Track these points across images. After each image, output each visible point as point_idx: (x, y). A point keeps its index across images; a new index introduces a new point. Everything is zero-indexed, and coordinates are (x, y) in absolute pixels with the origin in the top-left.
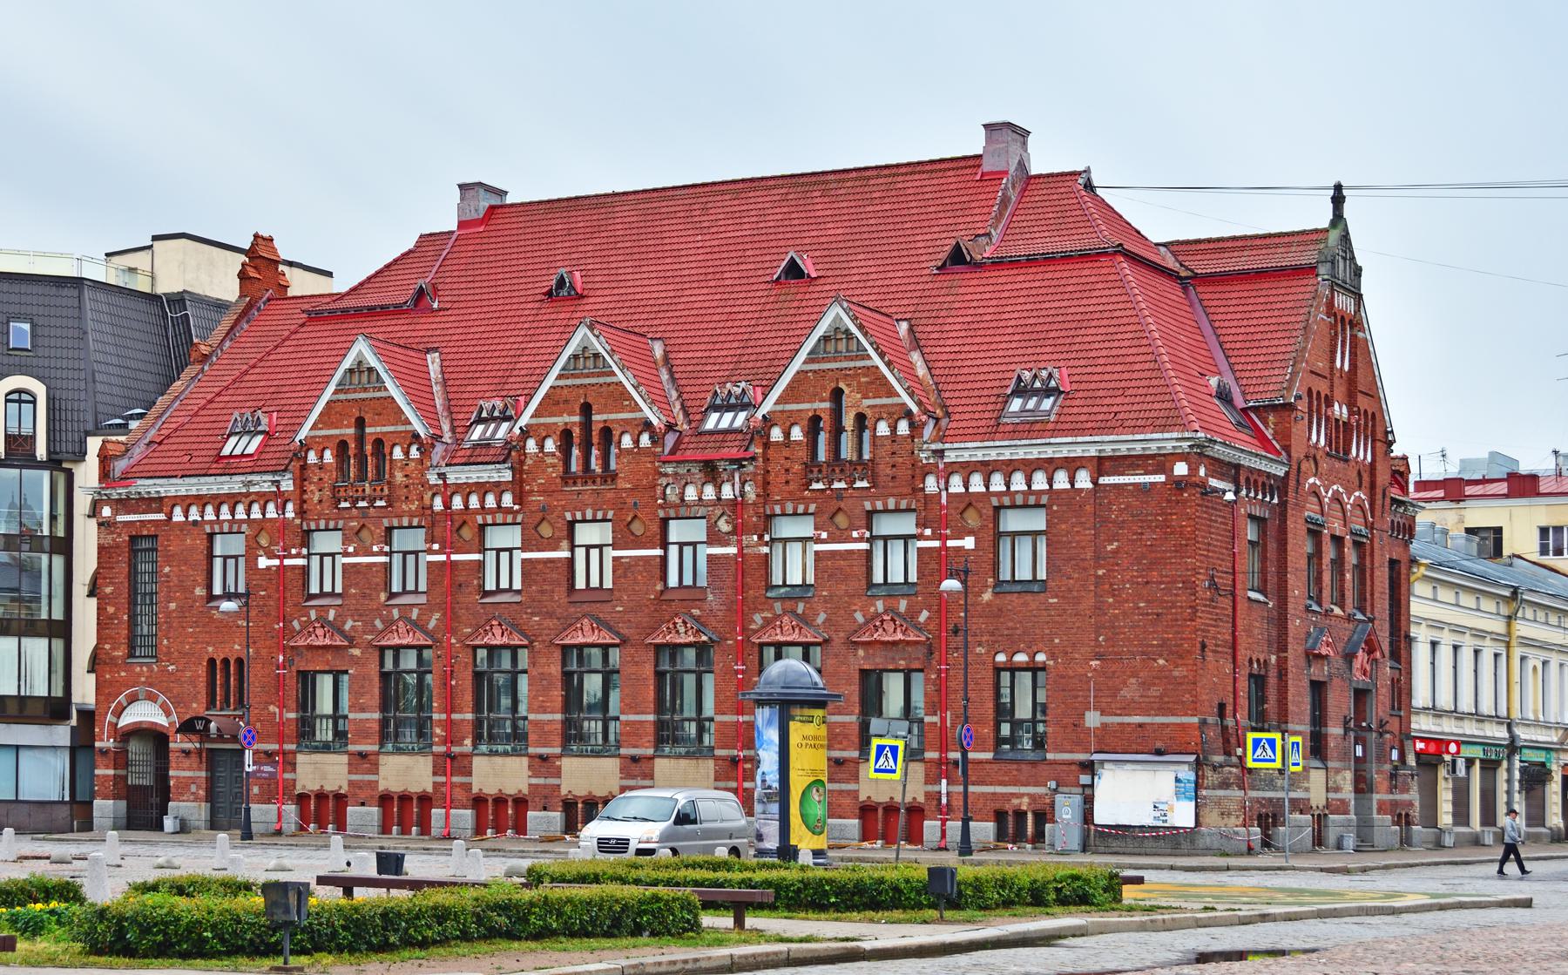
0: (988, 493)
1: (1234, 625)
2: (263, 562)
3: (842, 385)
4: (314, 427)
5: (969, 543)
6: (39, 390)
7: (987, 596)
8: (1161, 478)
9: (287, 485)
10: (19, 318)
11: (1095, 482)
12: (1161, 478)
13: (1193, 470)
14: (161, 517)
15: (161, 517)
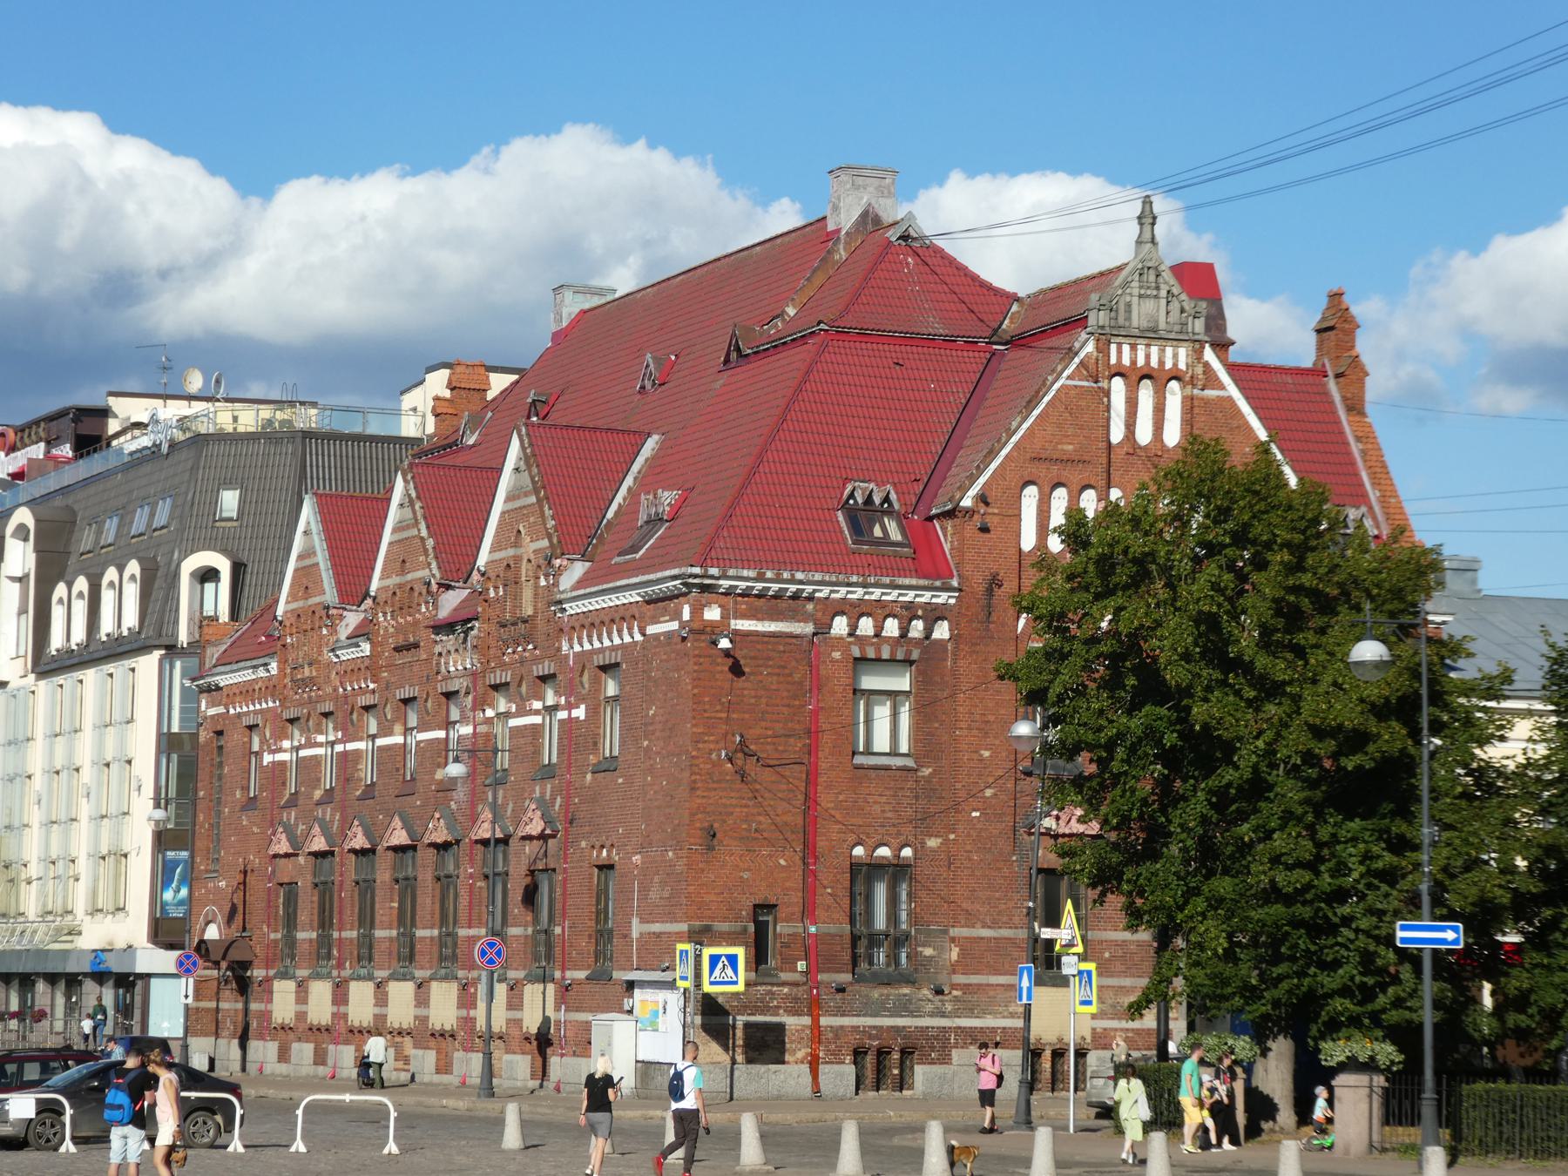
0: (593, 652)
1: (810, 800)
2: (267, 758)
3: (521, 529)
4: (287, 602)
5: (580, 713)
6: (223, 565)
7: (589, 776)
8: (674, 625)
9: (274, 666)
10: (229, 484)
11: (644, 634)
12: (674, 625)
13: (697, 611)
14: (221, 710)
15: (221, 710)
